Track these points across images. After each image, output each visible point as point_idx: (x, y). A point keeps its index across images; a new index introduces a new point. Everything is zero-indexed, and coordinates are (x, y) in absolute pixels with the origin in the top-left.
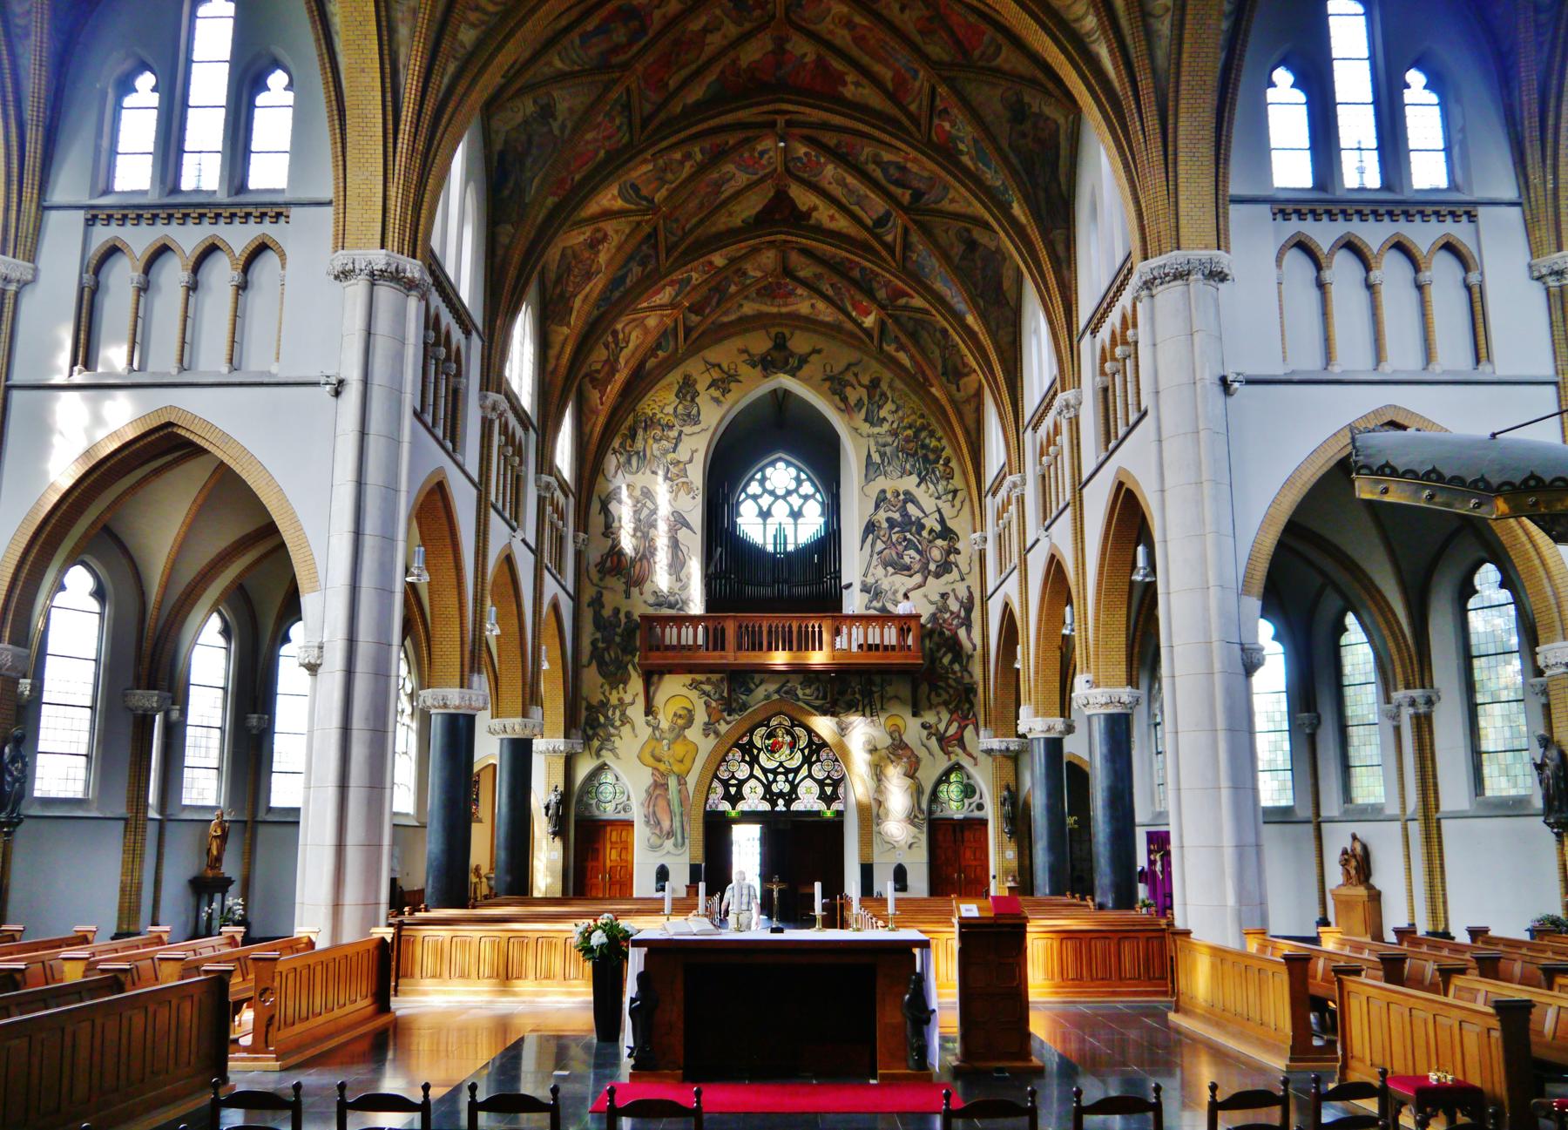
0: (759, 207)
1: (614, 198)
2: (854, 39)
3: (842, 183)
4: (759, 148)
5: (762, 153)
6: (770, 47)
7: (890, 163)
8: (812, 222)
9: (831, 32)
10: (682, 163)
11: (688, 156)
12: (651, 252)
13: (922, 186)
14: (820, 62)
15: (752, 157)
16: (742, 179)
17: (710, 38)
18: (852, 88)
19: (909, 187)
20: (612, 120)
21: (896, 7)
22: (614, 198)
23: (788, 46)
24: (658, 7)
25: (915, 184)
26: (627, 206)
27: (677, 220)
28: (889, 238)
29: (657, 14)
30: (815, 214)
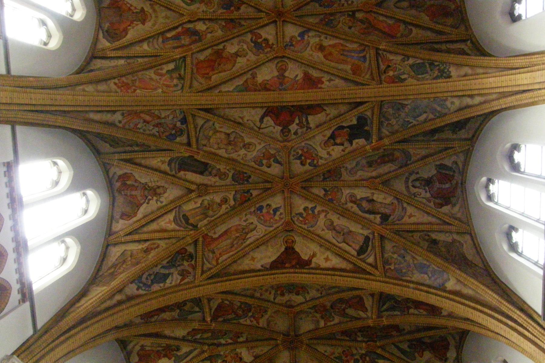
0: (273, 258)
1: (170, 222)
2: (325, 56)
3: (331, 227)
4: (274, 206)
5: (276, 210)
6: (276, 74)
7: (362, 199)
8: (313, 265)
9: (311, 55)
10: (220, 205)
11: (225, 200)
12: (190, 270)
13: (387, 211)
14: (307, 76)
15: (268, 212)
16: (261, 230)
17: (239, 59)
18: (327, 83)
19: (378, 213)
20: (172, 78)
21: (347, 29)
22: (170, 222)
23: (286, 74)
24: (211, 33)
25: (382, 210)
26: (177, 228)
27: (213, 252)
28: (371, 260)
29: (209, 36)
30: (314, 260)
